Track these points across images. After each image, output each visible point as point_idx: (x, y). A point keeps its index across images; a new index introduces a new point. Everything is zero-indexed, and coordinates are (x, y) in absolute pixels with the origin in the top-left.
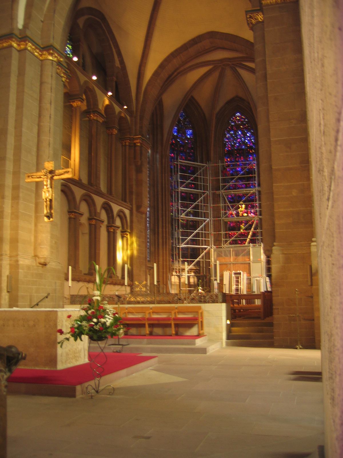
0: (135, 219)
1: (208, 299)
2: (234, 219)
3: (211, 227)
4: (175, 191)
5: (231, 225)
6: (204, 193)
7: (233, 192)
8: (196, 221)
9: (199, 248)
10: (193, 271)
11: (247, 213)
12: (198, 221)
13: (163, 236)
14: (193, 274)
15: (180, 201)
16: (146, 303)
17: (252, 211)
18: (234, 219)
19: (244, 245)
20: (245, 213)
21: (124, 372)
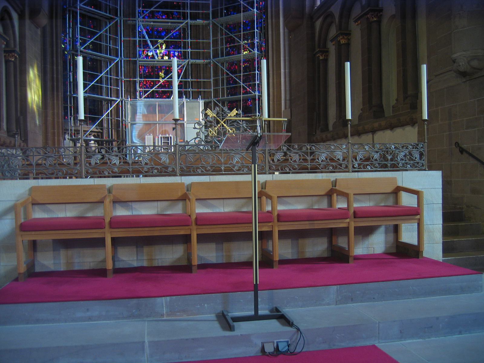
0: (28, 33)
1: (402, 160)
2: (155, 61)
3: (123, 69)
4: (69, 11)
5: (145, 71)
6: (112, 19)
7: (154, 22)
8: (97, 60)
9: (101, 100)
10: (93, 134)
11: (169, 55)
12: (101, 61)
13: (53, 77)
14: (92, 138)
15: (79, 26)
16: (239, 170)
17: (176, 54)
18: (155, 61)
19: (170, 100)
20: (166, 55)
21: (30, 306)
